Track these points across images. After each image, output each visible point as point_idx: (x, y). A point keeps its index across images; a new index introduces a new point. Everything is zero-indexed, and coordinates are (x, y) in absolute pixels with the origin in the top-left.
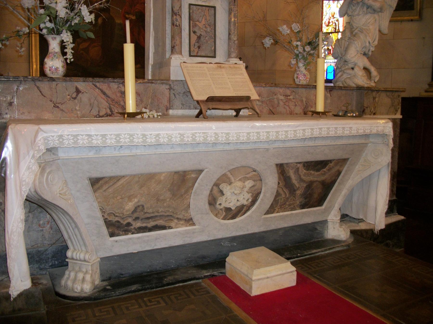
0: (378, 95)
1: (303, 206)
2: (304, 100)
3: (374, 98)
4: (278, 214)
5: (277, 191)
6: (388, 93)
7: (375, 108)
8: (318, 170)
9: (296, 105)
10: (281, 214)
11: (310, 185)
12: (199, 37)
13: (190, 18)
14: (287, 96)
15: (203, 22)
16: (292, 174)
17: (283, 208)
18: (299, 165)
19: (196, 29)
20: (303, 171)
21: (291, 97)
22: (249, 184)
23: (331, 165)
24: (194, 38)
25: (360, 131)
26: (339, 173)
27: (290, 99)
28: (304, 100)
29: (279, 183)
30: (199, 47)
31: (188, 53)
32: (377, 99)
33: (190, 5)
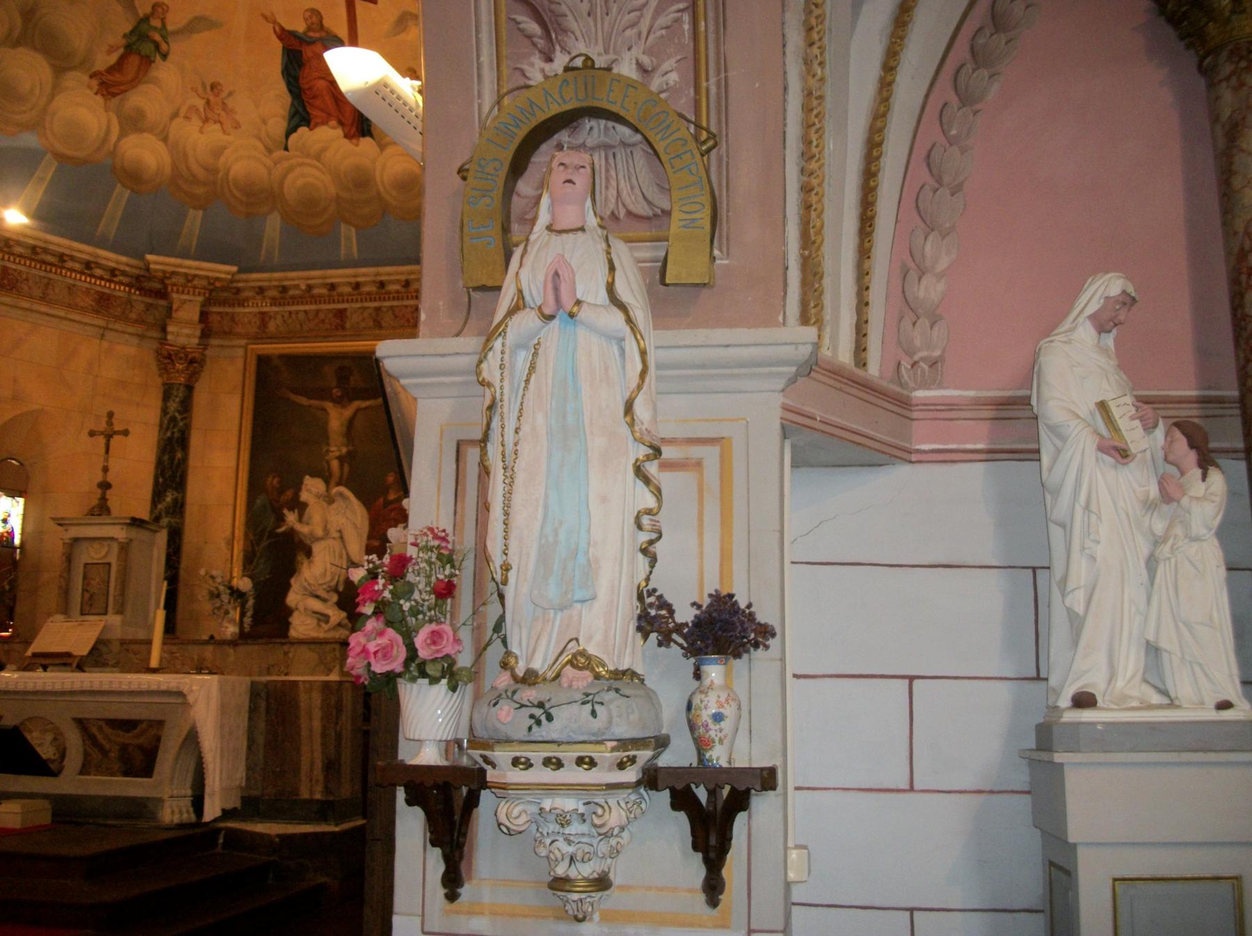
0: (292, 649)
1: (126, 774)
2: (196, 657)
3: (286, 654)
4: (95, 777)
5: (85, 750)
6: (313, 646)
7: (288, 666)
8: (128, 731)
9: (183, 664)
10: (98, 777)
11: (124, 748)
12: (91, 596)
13: (85, 577)
14: (173, 653)
15: (98, 580)
16: (94, 730)
17: (99, 770)
18: (100, 723)
19: (89, 589)
20: (108, 730)
21: (178, 655)
22: (49, 737)
23: (144, 726)
24: (87, 595)
25: (143, 686)
26: (158, 739)
27: (176, 658)
28: (196, 657)
29: (84, 741)
30: (91, 605)
31: (78, 612)
32: (291, 655)
33: (86, 564)
